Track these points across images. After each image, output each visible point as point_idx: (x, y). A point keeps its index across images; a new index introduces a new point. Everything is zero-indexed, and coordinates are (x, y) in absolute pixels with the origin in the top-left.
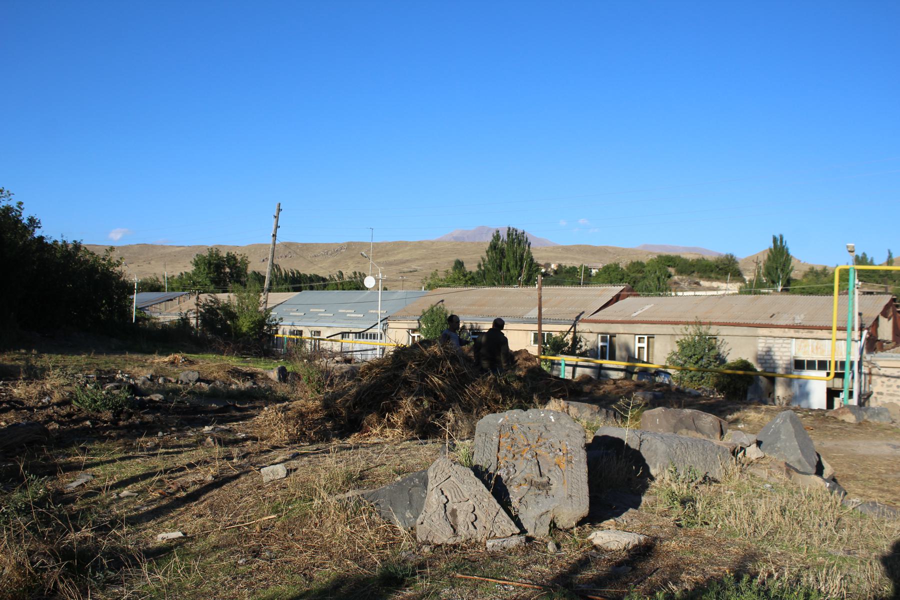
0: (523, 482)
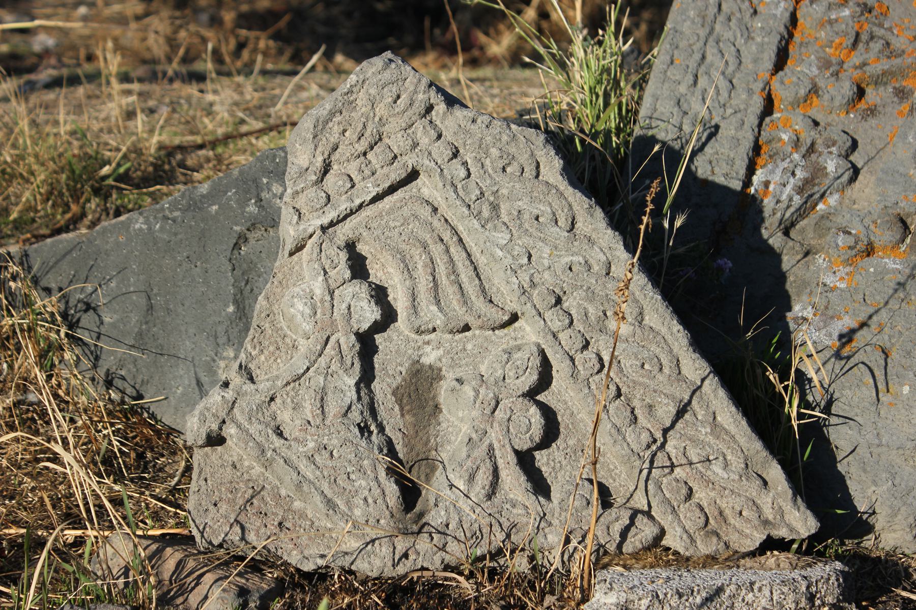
0: (884, 236)
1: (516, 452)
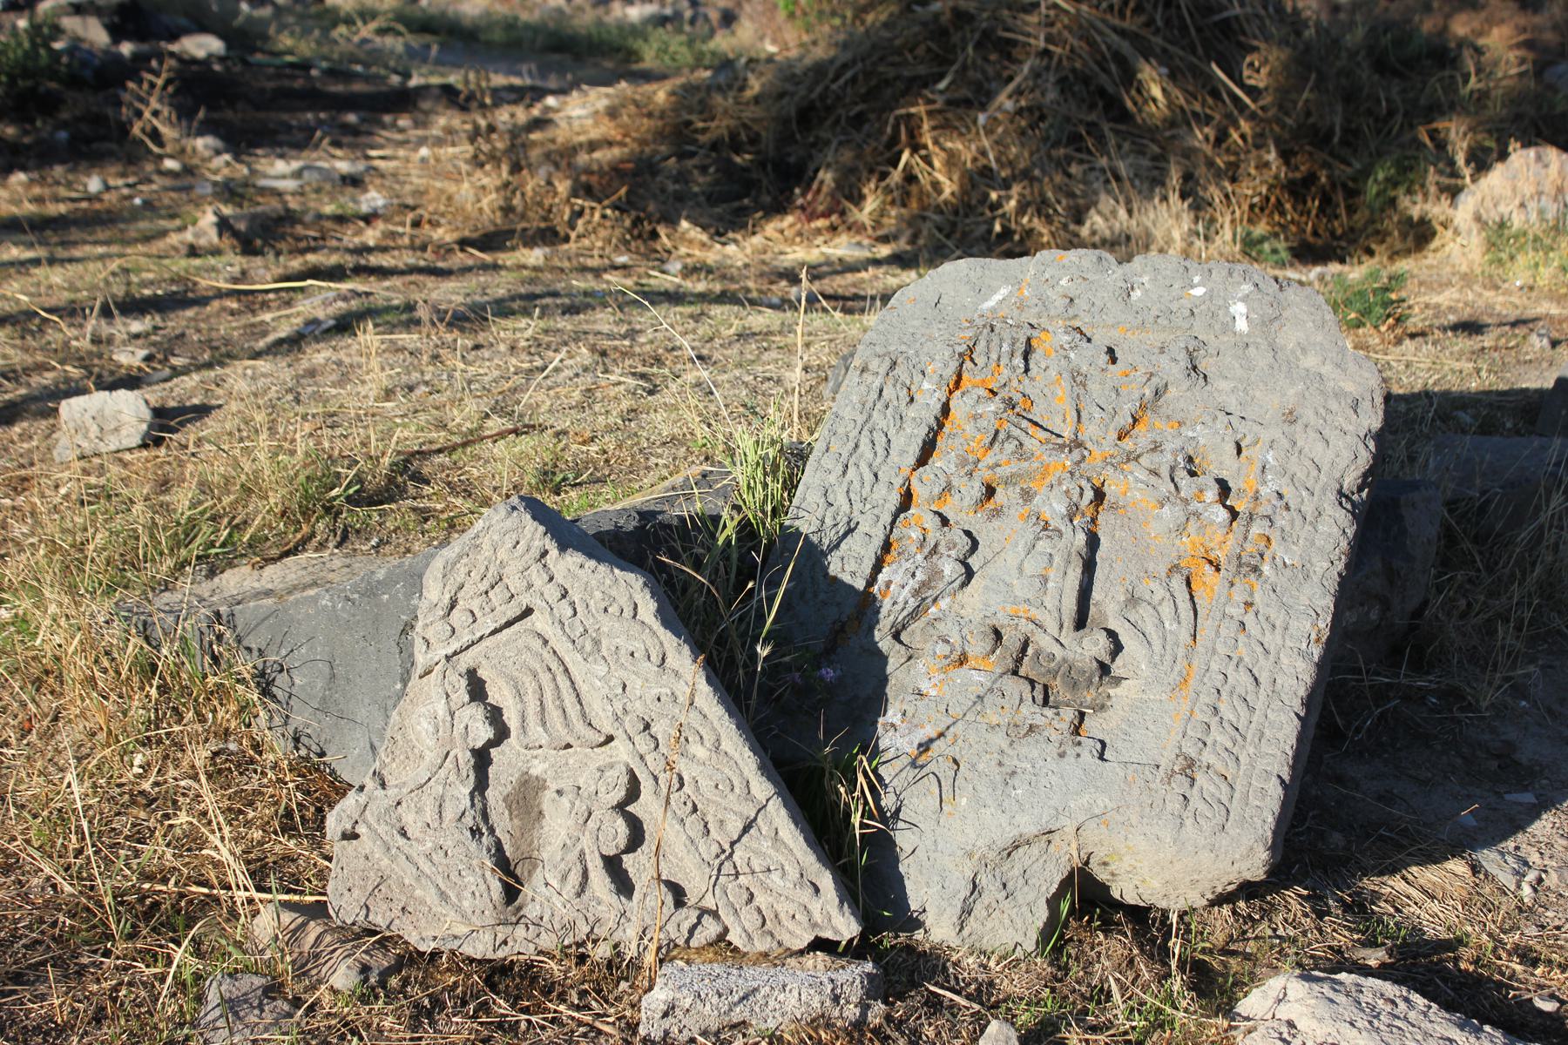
1: (604, 857)
